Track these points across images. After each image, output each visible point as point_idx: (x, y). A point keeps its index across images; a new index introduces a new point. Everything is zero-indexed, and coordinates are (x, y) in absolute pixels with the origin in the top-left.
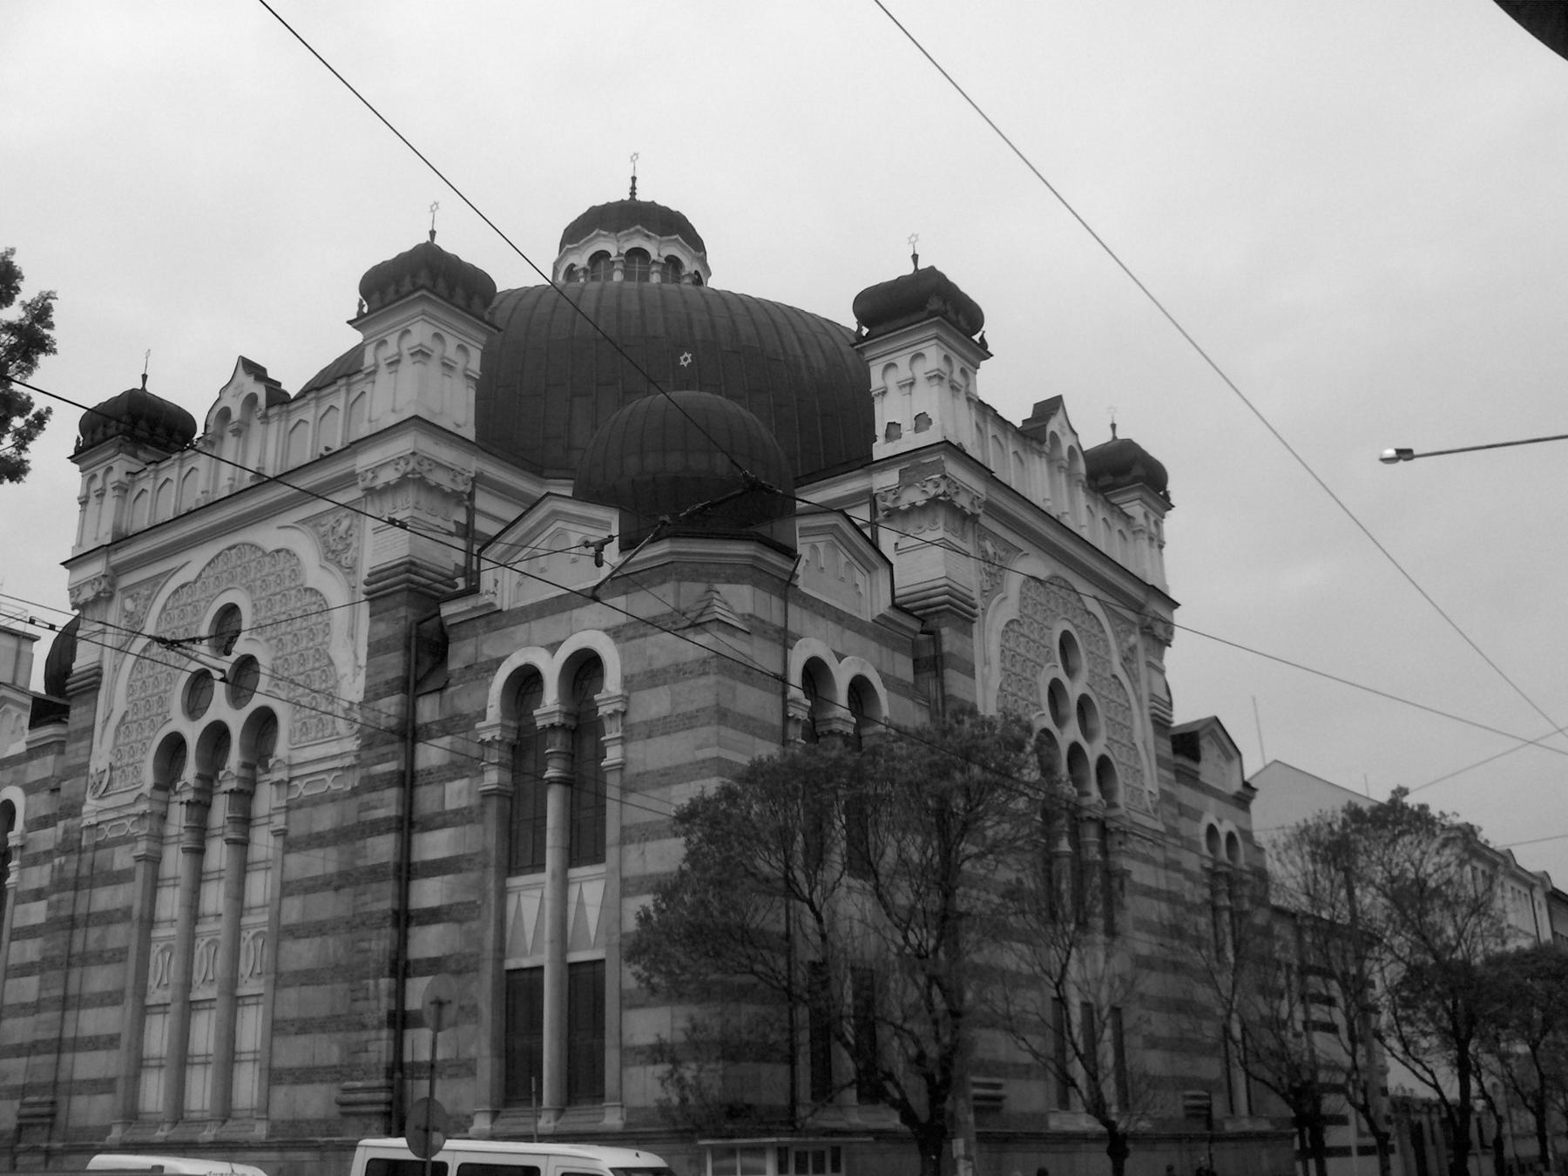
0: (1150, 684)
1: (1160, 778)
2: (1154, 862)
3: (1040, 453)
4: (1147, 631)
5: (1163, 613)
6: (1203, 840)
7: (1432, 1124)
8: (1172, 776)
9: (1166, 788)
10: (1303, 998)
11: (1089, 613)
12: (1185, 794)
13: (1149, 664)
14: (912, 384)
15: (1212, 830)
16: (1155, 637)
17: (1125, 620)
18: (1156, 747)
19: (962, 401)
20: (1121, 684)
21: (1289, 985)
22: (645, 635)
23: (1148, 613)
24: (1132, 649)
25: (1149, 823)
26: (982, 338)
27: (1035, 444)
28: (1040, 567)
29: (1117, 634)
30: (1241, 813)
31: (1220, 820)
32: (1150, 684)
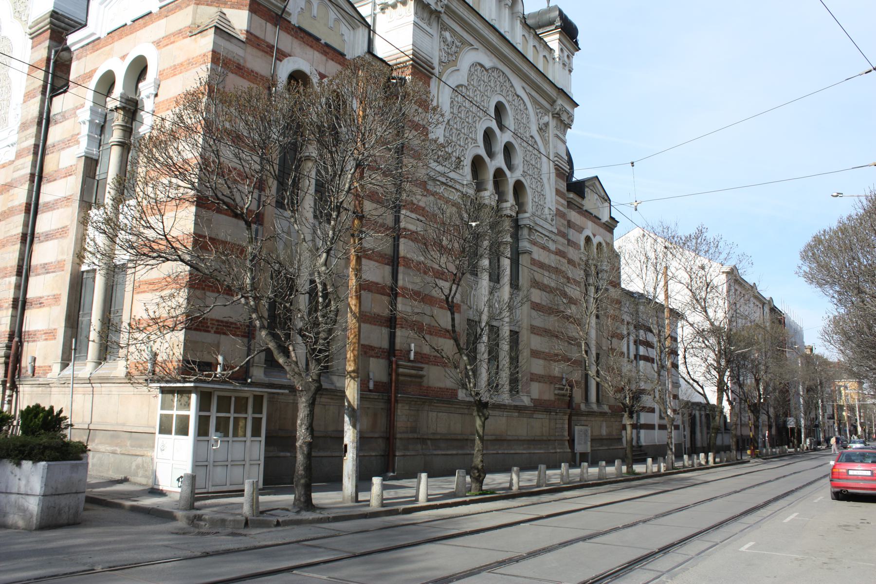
0: (555, 147)
1: (557, 202)
2: (549, 250)
4: (557, 116)
5: (568, 108)
6: (582, 243)
7: (701, 416)
8: (566, 203)
9: (561, 208)
10: (635, 342)
11: (518, 96)
12: (574, 216)
13: (557, 136)
15: (588, 240)
16: (562, 121)
17: (542, 107)
20: (535, 142)
21: (629, 334)
22: (174, 42)
23: (559, 106)
24: (547, 125)
28: (488, 61)
31: (594, 236)
32: (555, 147)
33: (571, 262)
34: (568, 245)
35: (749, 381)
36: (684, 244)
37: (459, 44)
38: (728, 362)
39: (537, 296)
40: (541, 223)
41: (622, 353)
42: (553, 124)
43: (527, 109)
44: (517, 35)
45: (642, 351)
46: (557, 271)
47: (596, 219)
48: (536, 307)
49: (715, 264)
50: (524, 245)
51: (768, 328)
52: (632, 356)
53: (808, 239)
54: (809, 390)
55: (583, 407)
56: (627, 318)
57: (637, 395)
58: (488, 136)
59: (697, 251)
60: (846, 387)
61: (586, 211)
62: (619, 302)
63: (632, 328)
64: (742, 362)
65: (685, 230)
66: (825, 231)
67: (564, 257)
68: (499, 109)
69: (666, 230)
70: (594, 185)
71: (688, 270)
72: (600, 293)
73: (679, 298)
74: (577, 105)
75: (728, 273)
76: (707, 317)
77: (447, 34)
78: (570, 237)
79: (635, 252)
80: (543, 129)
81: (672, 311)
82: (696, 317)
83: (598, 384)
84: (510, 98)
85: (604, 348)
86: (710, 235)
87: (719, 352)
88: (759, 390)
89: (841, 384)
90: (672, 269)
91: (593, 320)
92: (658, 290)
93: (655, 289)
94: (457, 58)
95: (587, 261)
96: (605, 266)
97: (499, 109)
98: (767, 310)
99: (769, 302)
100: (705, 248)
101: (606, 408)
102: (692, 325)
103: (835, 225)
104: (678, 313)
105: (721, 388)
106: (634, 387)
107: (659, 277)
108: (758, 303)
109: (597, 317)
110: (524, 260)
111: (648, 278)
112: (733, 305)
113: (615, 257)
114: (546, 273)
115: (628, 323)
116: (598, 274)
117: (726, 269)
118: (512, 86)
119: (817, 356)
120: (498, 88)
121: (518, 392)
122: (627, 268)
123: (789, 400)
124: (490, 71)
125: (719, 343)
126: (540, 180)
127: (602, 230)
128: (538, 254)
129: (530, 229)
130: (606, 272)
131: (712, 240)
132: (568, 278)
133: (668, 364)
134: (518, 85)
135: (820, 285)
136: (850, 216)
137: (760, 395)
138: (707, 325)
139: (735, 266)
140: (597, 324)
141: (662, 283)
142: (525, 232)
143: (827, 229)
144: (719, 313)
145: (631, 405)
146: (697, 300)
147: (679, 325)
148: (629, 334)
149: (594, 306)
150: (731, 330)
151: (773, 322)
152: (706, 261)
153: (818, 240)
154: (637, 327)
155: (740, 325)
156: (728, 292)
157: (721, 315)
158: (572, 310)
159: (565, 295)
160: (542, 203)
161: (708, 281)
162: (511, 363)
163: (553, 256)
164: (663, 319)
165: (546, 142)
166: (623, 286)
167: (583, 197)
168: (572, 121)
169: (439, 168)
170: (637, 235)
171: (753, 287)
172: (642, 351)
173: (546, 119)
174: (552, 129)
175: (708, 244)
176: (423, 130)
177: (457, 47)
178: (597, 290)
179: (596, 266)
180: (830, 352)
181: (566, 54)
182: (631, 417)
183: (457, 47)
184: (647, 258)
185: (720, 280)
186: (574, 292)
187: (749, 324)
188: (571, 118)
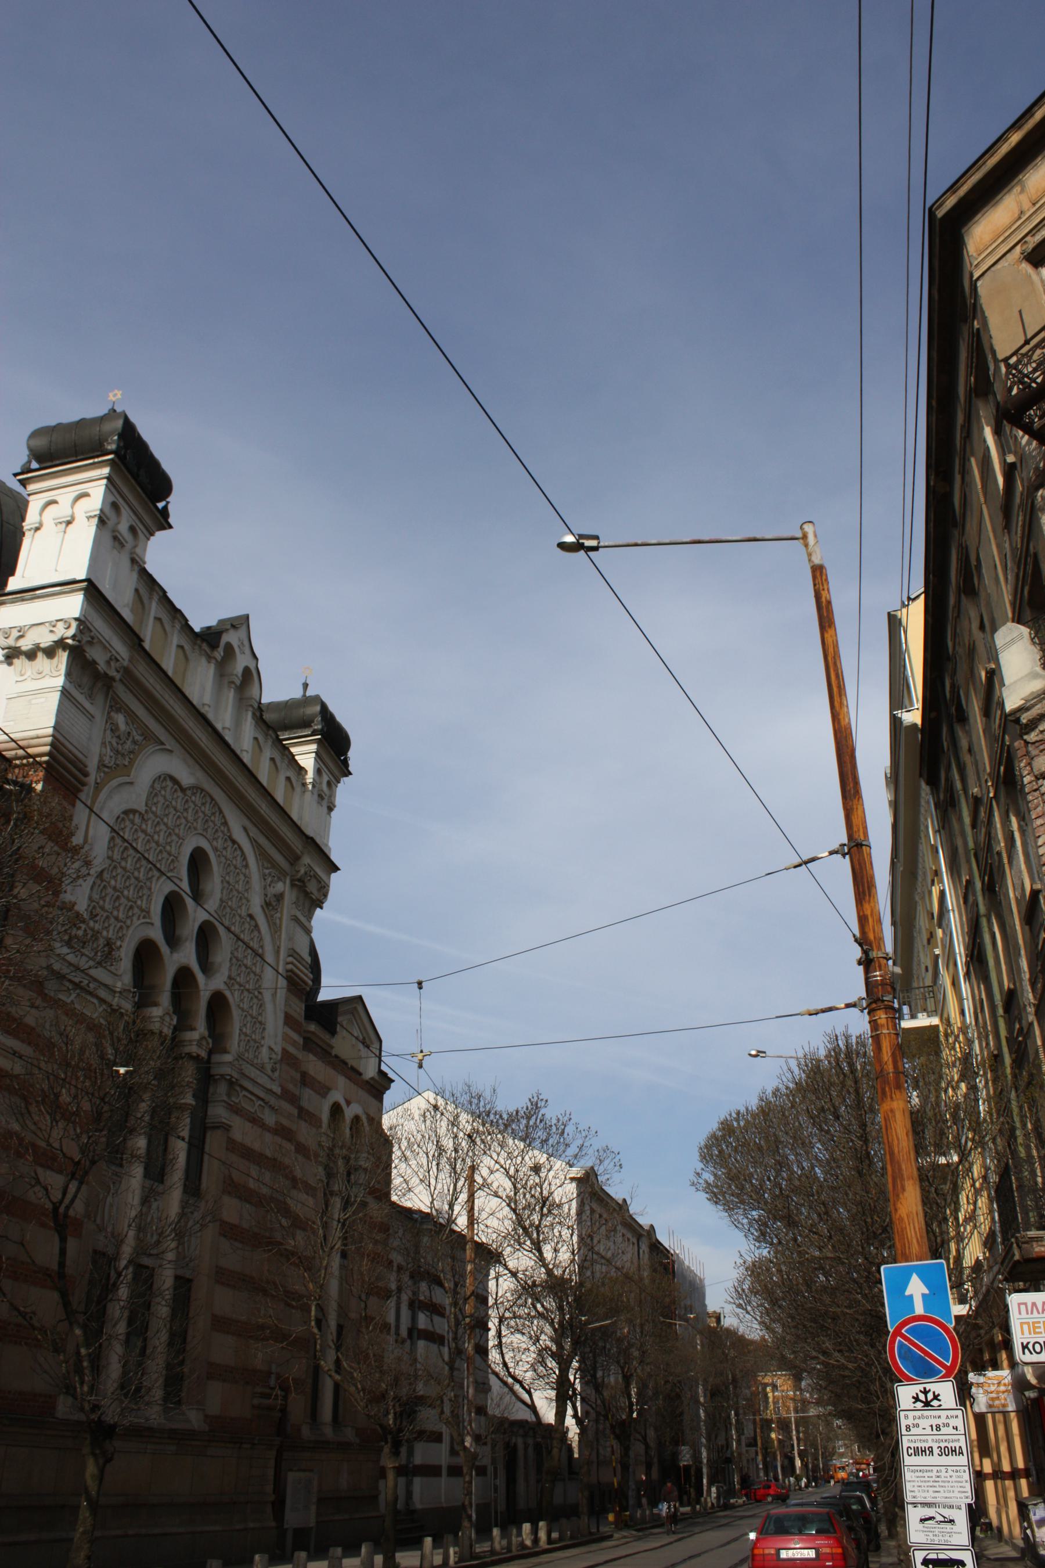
0: (291, 939)
1: (286, 1037)
2: (263, 1126)
3: (209, 658)
4: (299, 884)
6: (325, 1116)
7: (526, 1448)
8: (301, 1041)
9: (291, 1049)
10: (411, 1305)
11: (234, 842)
12: (315, 1066)
13: (296, 920)
14: (69, 523)
15: (336, 1110)
16: (307, 894)
17: (273, 864)
18: (287, 1003)
19: (126, 562)
20: (257, 926)
21: (399, 1289)
23: (305, 870)
24: (279, 897)
25: (263, 1080)
26: (165, 508)
27: (205, 646)
28: (186, 774)
29: (264, 877)
30: (374, 1102)
31: (348, 1103)
32: (291, 939)
33: (301, 1149)
34: (300, 1116)
35: (612, 1379)
36: (506, 1126)
37: (138, 738)
38: (575, 1343)
39: (233, 1210)
40: (253, 1073)
41: (386, 1327)
42: (290, 896)
43: (247, 866)
44: (245, 738)
45: (423, 1321)
46: (274, 1165)
47: (353, 1073)
48: (230, 1231)
49: (558, 1164)
50: (218, 1112)
51: (647, 1282)
52: (404, 1333)
53: (712, 1126)
54: (714, 1393)
55: (306, 1431)
56: (397, 1258)
57: (409, 1408)
58: (172, 907)
59: (527, 1139)
60: (775, 1387)
61: (336, 1056)
62: (384, 1228)
63: (406, 1278)
64: (601, 1344)
65: (509, 1102)
66: (738, 1113)
67: (290, 1140)
68: (198, 862)
69: (475, 1101)
70: (353, 1012)
71: (512, 1172)
72: (351, 1210)
73: (493, 1221)
74: (336, 869)
75: (578, 1181)
76: (541, 1258)
77: (120, 719)
78: (305, 1104)
79: (419, 1137)
80: (272, 904)
81: (480, 1247)
82: (521, 1260)
83: (337, 1386)
84: (219, 844)
85: (353, 1315)
86: (550, 1113)
87: (560, 1323)
88: (629, 1396)
89: (766, 1381)
90: (485, 1172)
91: (336, 1261)
92: (457, 1208)
93: (451, 1206)
94: (132, 762)
95: (331, 1149)
96: (364, 1161)
97: (198, 862)
98: (644, 1247)
99: (648, 1232)
100: (541, 1134)
101: (349, 1434)
102: (514, 1274)
103: (754, 1103)
104: (490, 1252)
105: (563, 1395)
106: (404, 1391)
107: (460, 1184)
108: (629, 1235)
109: (344, 1255)
110: (214, 1142)
111: (439, 1186)
112: (586, 1241)
113: (383, 1144)
114: (254, 1171)
115: (400, 1268)
116: (349, 1174)
117: (576, 1172)
118: (225, 824)
119: (728, 1330)
120: (199, 825)
121: (179, 1403)
122: (403, 1165)
123: (682, 1414)
124: (189, 793)
125: (560, 1308)
126: (256, 994)
127: (363, 1094)
128: (242, 1131)
129: (232, 1083)
130: (365, 1170)
131: (554, 1121)
132: (294, 1181)
133: (469, 1347)
134: (236, 824)
135: (729, 1209)
136: (778, 1090)
137: (631, 1404)
138: (541, 1274)
139: (592, 1168)
140: (342, 1267)
141: (463, 1197)
142: (222, 1088)
143: (743, 1110)
144: (562, 1252)
145: (396, 1429)
146: (524, 1229)
147: (492, 1274)
148: (399, 1289)
149: (339, 1234)
150: (581, 1284)
151: (655, 1270)
152: (542, 1158)
153: (727, 1128)
154: (417, 1275)
155: (598, 1275)
156: (580, 1213)
157: (564, 1256)
158: (298, 1241)
159: (287, 1211)
160: (257, 1037)
161: (545, 1193)
162: (170, 1344)
163: (268, 1137)
164: (464, 1262)
165: (275, 928)
166: (394, 1198)
167: (333, 1033)
168: (325, 895)
169: (70, 958)
170: (424, 1105)
171: (622, 1207)
172: (423, 1321)
173: (280, 887)
174: (288, 907)
175: (547, 1128)
176: (53, 884)
177: (135, 742)
178: (347, 1204)
179: (347, 1159)
180: (746, 1323)
181: (325, 778)
182: (396, 1453)
183: (135, 742)
184: (440, 1149)
185: (565, 1193)
186: (303, 1204)
187: (613, 1273)
188: (324, 890)
